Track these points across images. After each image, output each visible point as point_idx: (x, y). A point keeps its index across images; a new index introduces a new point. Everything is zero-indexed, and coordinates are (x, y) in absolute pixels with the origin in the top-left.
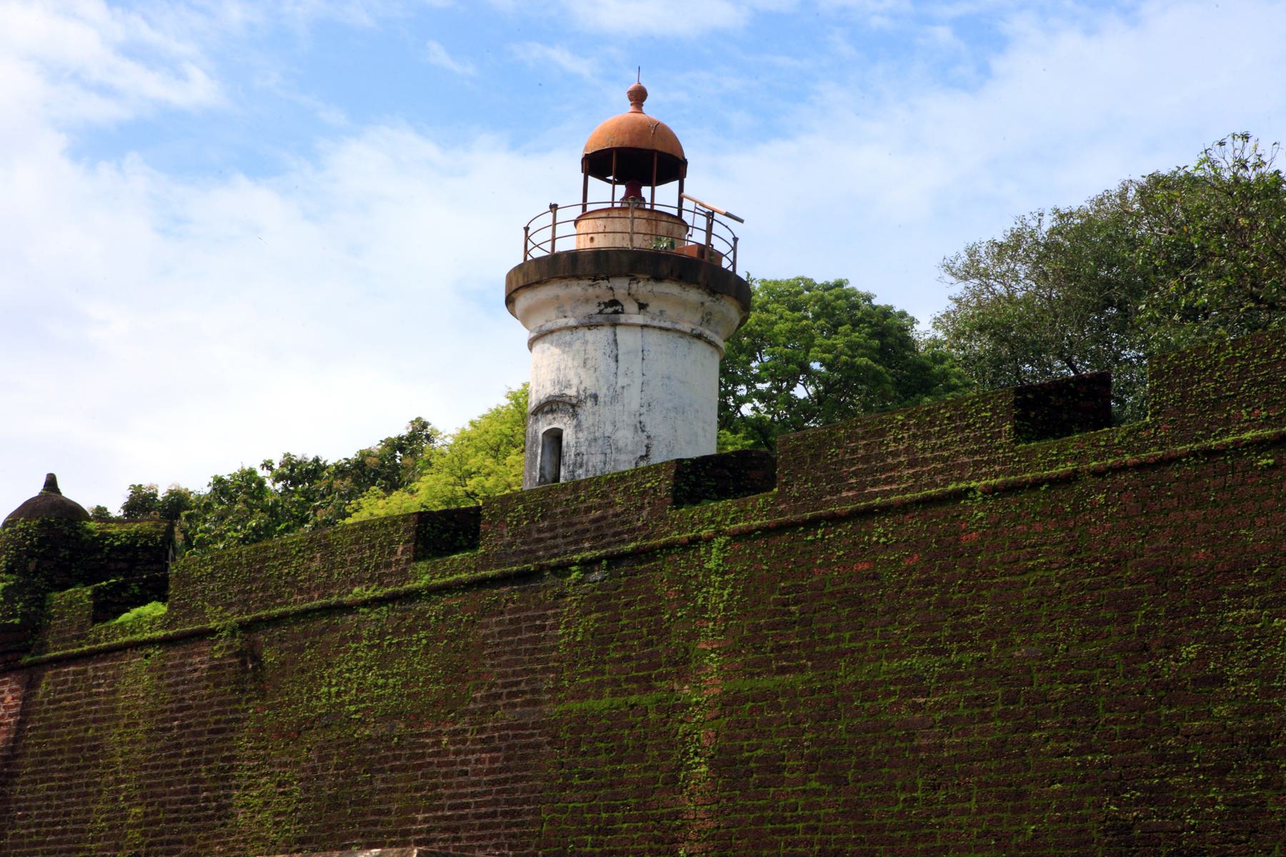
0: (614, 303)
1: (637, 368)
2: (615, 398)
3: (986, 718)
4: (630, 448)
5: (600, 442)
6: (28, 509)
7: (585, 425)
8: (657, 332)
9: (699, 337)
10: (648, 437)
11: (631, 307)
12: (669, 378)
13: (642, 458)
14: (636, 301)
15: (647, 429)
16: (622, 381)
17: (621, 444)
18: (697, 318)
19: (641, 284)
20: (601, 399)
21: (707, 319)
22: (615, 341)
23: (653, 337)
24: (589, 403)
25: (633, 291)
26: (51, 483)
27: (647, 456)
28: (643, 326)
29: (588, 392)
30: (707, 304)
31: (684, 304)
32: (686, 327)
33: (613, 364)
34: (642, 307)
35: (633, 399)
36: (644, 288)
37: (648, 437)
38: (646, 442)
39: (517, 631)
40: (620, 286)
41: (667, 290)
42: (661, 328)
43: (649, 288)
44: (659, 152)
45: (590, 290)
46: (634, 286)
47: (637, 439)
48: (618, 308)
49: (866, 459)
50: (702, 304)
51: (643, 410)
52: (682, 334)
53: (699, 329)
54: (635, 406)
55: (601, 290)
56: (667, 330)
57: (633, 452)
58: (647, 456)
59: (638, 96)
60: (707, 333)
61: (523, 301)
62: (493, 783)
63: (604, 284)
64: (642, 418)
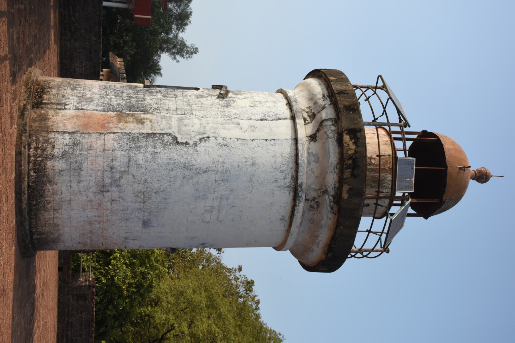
1: (258, 135)
4: (184, 128)
5: (187, 108)
7: (203, 100)
8: (294, 152)
9: (296, 197)
15: (203, 144)
16: (245, 124)
19: (333, 128)
20: (226, 109)
22: (279, 119)
23: (287, 149)
25: (325, 123)
28: (296, 140)
30: (326, 197)
32: (303, 179)
33: (259, 117)
35: (231, 132)
36: (330, 129)
37: (195, 144)
38: (191, 143)
40: (328, 113)
41: (332, 151)
42: (297, 155)
46: (330, 123)
47: (193, 134)
50: (325, 192)
52: (295, 178)
53: (303, 195)
54: (223, 133)
58: (178, 143)
59: (482, 177)
60: (301, 206)
63: (328, 102)
64: (211, 138)
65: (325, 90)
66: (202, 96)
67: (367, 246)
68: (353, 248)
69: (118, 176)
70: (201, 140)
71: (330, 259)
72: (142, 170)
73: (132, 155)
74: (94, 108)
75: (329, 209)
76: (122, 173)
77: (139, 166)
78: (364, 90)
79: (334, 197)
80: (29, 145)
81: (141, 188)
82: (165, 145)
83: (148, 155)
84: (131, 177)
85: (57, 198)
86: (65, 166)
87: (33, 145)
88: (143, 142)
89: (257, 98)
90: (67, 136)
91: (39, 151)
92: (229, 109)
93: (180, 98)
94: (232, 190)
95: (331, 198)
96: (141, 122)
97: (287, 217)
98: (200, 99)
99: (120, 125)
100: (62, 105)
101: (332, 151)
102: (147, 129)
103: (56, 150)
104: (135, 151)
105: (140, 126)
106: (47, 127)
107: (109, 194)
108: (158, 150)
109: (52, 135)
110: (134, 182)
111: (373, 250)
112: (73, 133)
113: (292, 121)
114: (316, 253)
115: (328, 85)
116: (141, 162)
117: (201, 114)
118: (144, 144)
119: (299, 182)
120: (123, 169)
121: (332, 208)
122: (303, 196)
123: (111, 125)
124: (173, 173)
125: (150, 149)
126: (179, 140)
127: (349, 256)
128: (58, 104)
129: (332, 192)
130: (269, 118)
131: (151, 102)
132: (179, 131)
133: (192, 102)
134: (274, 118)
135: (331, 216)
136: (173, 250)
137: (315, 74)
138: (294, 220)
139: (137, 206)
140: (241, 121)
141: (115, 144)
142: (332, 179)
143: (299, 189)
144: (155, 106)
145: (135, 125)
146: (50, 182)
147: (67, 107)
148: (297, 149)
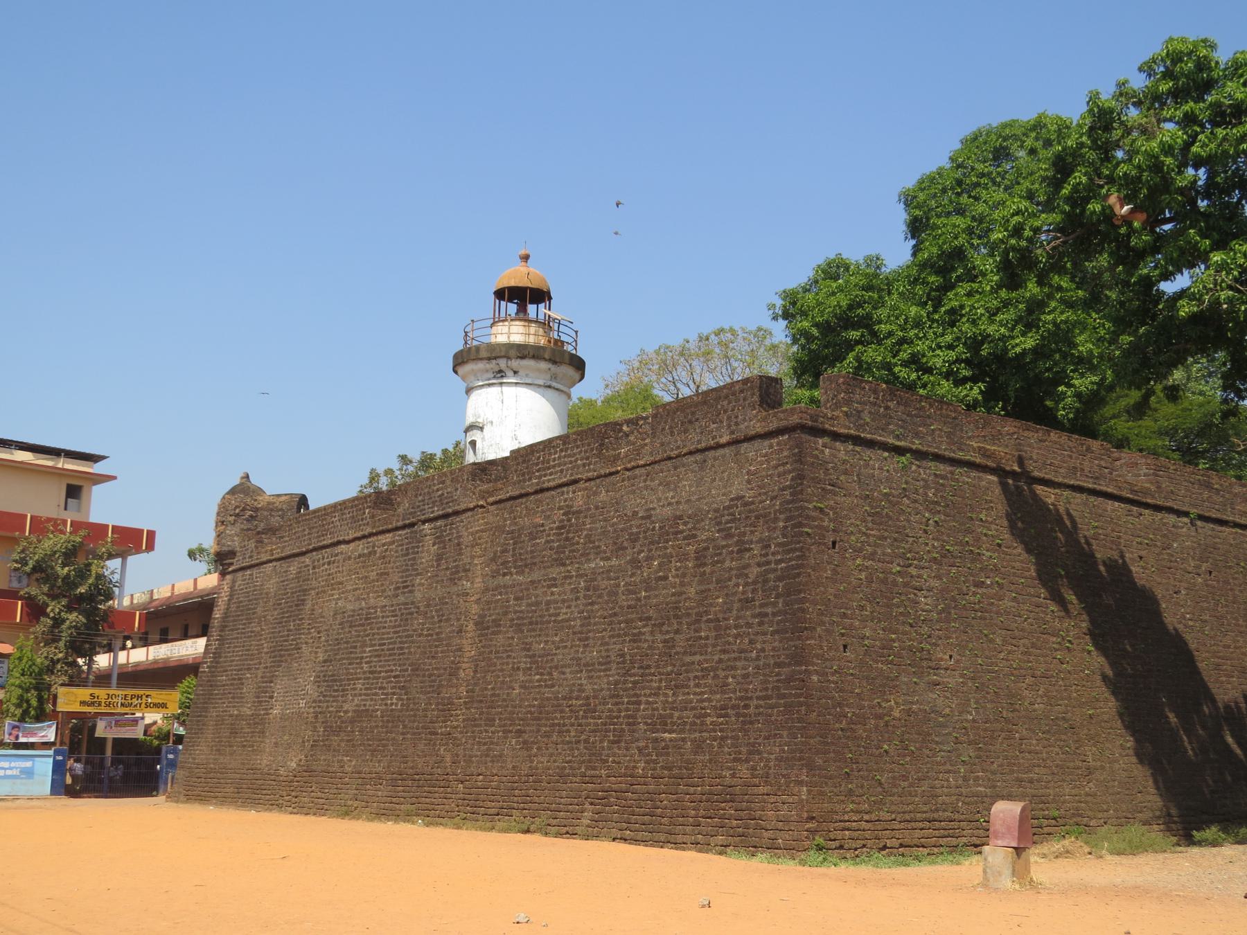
0: (500, 371)
3: (577, 599)
6: (233, 491)
9: (549, 387)
11: (510, 373)
18: (548, 376)
21: (554, 377)
26: (247, 477)
31: (539, 370)
32: (541, 382)
34: (515, 372)
36: (515, 363)
39: (407, 554)
40: (503, 363)
44: (531, 289)
49: (543, 462)
55: (493, 365)
60: (554, 384)
61: (461, 370)
62: (395, 632)
114: (577, 376)
129: (550, 366)
142: (543, 365)
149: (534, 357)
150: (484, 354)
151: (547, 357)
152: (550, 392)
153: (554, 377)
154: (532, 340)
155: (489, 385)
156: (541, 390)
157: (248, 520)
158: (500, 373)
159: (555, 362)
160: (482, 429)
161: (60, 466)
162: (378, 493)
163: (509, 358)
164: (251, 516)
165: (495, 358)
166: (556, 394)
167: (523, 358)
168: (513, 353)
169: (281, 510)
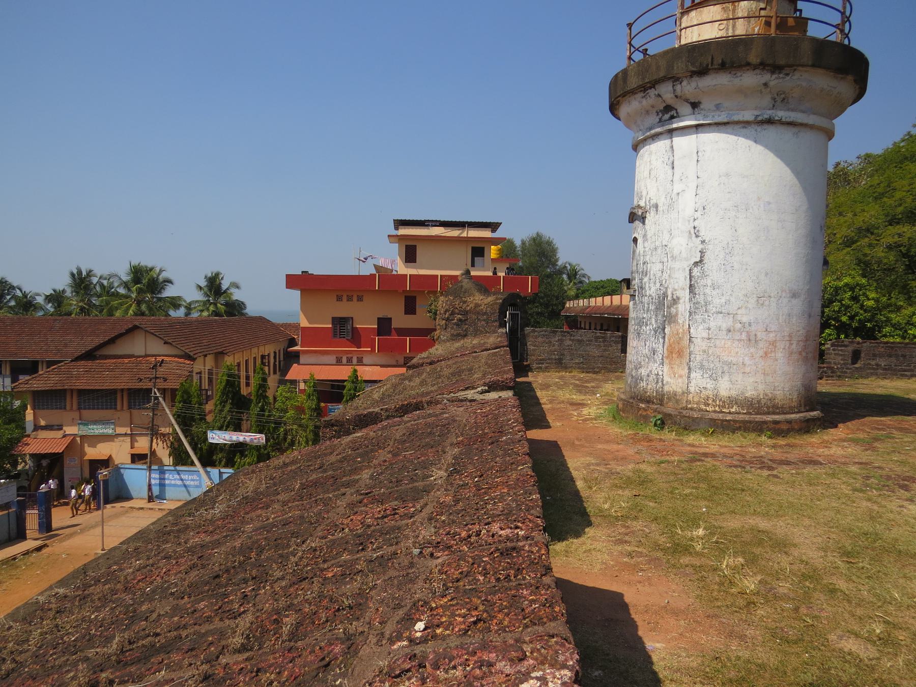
0: (668, 108)
2: (670, 207)
4: (684, 255)
5: (659, 251)
7: (649, 234)
8: (715, 128)
9: (770, 121)
10: (703, 242)
11: (685, 109)
12: (727, 175)
13: (696, 264)
14: (687, 101)
16: (678, 187)
17: (676, 252)
18: (767, 101)
19: (685, 83)
22: (672, 147)
24: (653, 212)
25: (679, 92)
27: (701, 261)
29: (652, 202)
30: (772, 84)
31: (742, 92)
32: (748, 116)
33: (670, 171)
34: (695, 105)
35: (687, 204)
36: (688, 87)
37: (703, 242)
38: (701, 247)
40: (666, 91)
41: (714, 82)
42: (717, 124)
43: (694, 85)
45: (644, 102)
46: (678, 87)
47: (691, 245)
48: (673, 113)
50: (766, 85)
51: (698, 214)
52: (746, 124)
53: (767, 114)
54: (689, 212)
55: (650, 100)
56: (725, 124)
57: (687, 259)
58: (701, 261)
60: (780, 114)
63: (652, 92)
64: (696, 224)
65: (636, 96)
66: (645, 236)
67: (836, 19)
68: (833, 38)
69: (738, 326)
70: (697, 236)
71: (850, 67)
72: (733, 299)
73: (714, 309)
74: (661, 347)
75: (788, 78)
76: (734, 321)
77: (728, 302)
78: (633, 50)
79: (773, 73)
80: (701, 410)
81: (753, 301)
82: (704, 275)
83: (714, 293)
84: (740, 312)
85: (761, 387)
86: (726, 378)
87: (703, 407)
88: (700, 299)
89: (646, 173)
90: (693, 375)
91: (710, 402)
92: (660, 205)
93: (647, 258)
94: (759, 199)
95: (774, 76)
96: (675, 301)
97: (795, 130)
98: (648, 237)
99: (680, 321)
100: (658, 379)
101: (714, 82)
102: (685, 295)
103: (708, 386)
104: (710, 307)
105: (681, 301)
106: (683, 393)
107: (759, 334)
108: (709, 283)
109: (692, 389)
110: (746, 308)
111: (843, 13)
112: (689, 369)
113: (674, 133)
114: (844, 87)
115: (629, 93)
116: (723, 300)
117: (666, 236)
118: (702, 297)
119: (751, 118)
120: (731, 319)
121: (787, 75)
122: (770, 112)
123: (681, 330)
124: (736, 266)
125: (708, 291)
126: (698, 259)
127: (846, 42)
128: (657, 382)
129: (767, 77)
130: (671, 159)
131: (653, 289)
132: (687, 259)
133: (653, 246)
134: (670, 154)
135: (797, 75)
136: (826, 262)
137: (614, 108)
138: (800, 121)
139: (774, 305)
140: (675, 192)
141: (701, 327)
142: (750, 79)
143: (760, 118)
144: (658, 285)
145: (679, 306)
146: (743, 393)
147: (660, 373)
148: (709, 124)
149: (723, 67)
150: (633, 82)
151: (753, 59)
152: (771, 132)
153: (781, 99)
154: (741, 29)
155: (655, 137)
156: (750, 130)
157: (457, 325)
158: (668, 112)
159: (776, 69)
160: (643, 219)
161: (464, 235)
162: (562, 298)
163: (676, 79)
164: (460, 320)
165: (654, 84)
166: (787, 134)
167: (702, 72)
168: (680, 67)
169: (485, 313)
